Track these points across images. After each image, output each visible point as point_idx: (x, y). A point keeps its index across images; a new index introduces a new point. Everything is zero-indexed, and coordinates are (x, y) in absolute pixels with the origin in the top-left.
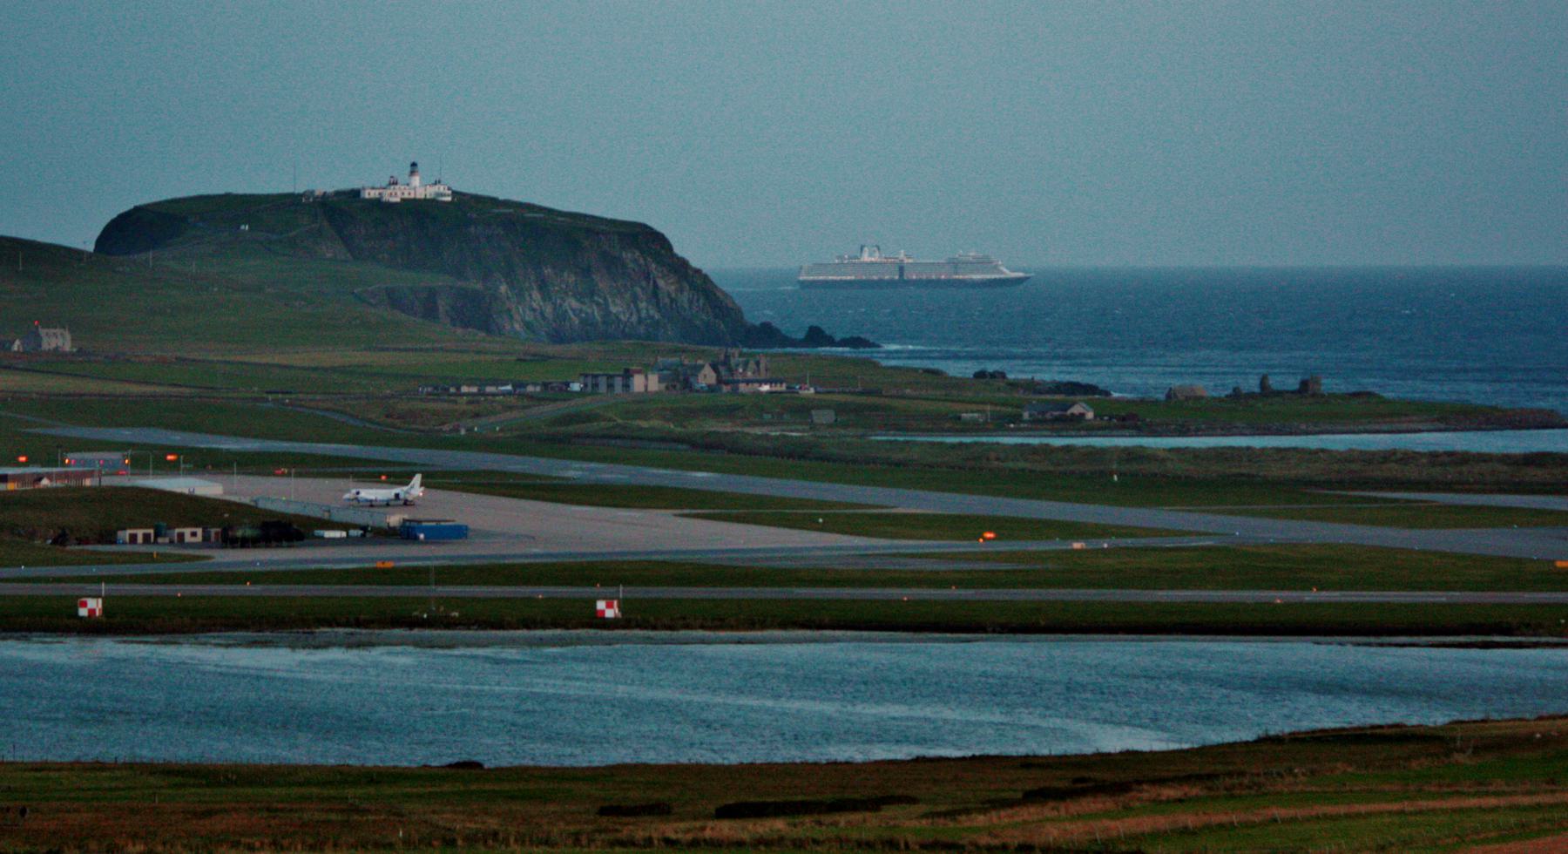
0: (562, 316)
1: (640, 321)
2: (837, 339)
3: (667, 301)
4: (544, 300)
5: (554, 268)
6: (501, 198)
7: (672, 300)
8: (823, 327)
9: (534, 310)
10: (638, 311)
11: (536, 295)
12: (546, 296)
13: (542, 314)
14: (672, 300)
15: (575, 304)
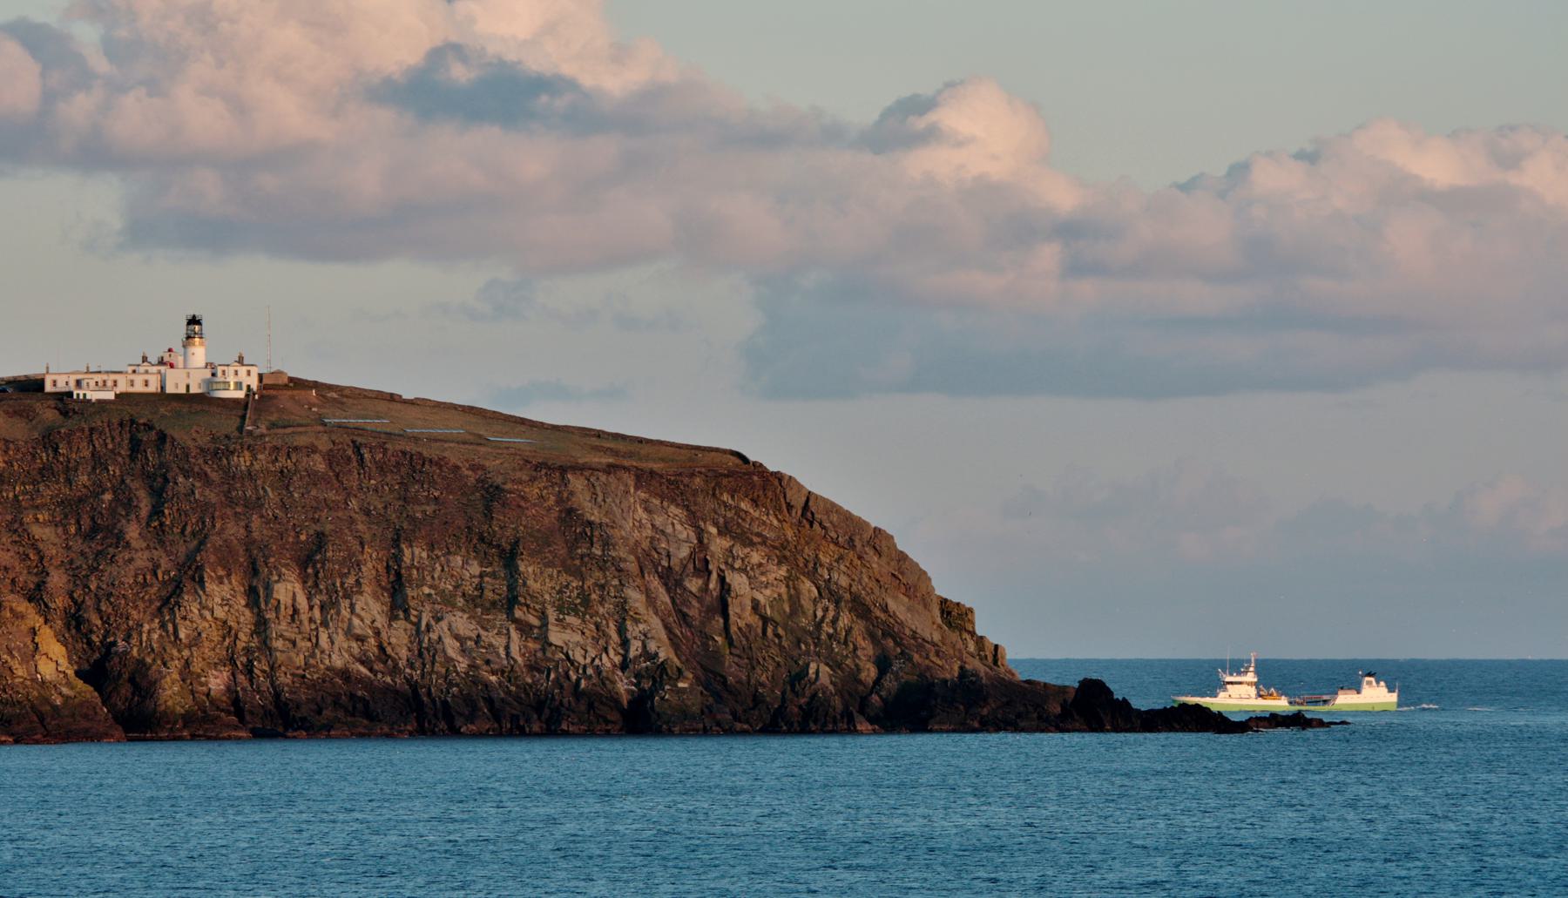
0: (425, 652)
1: (624, 666)
2: (1140, 703)
3: (755, 621)
4: (393, 618)
5: (431, 547)
6: (406, 396)
7: (765, 620)
8: (1112, 687)
9: (361, 639)
10: (625, 643)
11: (370, 608)
12: (398, 605)
13: (381, 648)
14: (765, 620)
15: (462, 623)
